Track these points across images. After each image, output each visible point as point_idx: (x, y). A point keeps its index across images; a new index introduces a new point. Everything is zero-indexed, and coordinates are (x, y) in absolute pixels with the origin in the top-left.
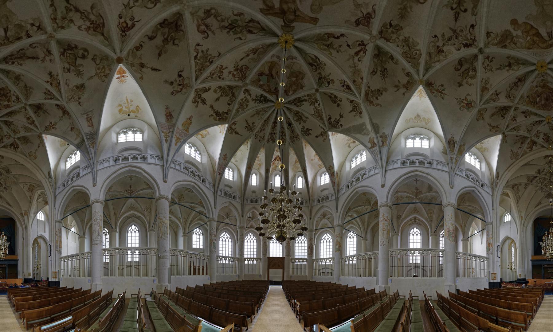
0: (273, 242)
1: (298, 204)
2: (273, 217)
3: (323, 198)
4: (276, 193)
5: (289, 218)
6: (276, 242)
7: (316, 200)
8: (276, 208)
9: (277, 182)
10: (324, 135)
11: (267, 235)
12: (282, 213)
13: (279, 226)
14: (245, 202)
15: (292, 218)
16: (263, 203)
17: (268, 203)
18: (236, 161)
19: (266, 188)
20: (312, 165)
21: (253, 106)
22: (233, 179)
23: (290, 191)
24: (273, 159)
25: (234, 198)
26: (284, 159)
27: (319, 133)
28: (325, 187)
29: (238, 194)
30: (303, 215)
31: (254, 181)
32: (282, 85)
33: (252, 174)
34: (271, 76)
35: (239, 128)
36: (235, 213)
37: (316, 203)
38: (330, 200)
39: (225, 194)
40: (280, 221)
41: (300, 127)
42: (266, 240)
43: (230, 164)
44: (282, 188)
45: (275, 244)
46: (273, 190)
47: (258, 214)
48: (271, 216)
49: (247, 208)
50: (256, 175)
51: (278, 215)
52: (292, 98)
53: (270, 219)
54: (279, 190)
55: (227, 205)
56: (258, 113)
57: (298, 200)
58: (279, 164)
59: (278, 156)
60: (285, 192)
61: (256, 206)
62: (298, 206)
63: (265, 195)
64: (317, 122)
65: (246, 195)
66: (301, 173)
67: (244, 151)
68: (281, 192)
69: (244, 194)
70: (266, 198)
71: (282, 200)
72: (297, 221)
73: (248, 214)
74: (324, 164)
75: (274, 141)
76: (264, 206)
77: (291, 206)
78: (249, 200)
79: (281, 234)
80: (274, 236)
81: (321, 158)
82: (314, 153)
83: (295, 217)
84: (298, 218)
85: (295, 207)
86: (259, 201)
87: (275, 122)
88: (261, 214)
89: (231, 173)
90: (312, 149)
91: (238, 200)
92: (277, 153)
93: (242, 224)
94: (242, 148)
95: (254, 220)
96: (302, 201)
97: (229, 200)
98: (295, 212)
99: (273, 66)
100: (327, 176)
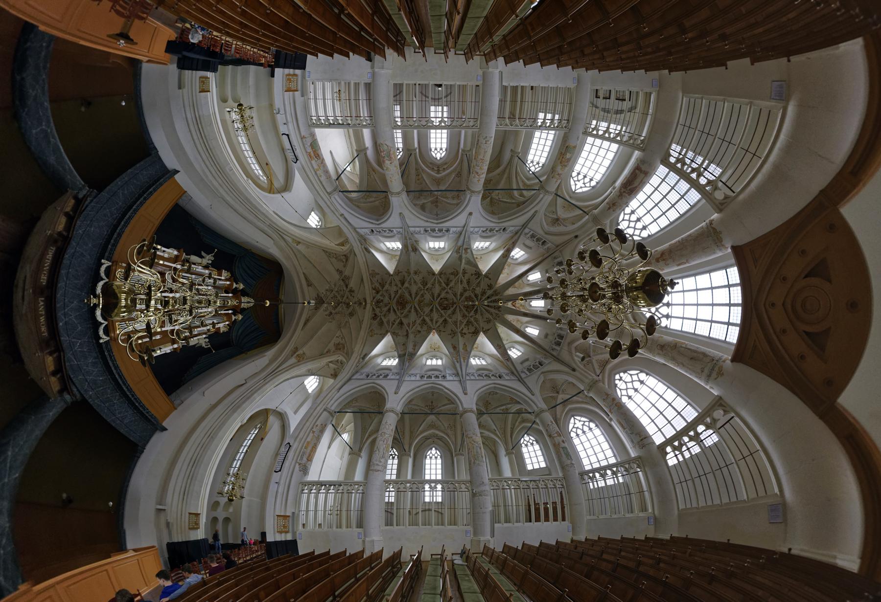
0: (667, 316)
1: (564, 269)
2: (595, 312)
3: (537, 241)
4: (552, 305)
5: (593, 278)
6: (668, 305)
7: (546, 247)
8: (577, 305)
9: (538, 304)
10: (486, 276)
11: (639, 333)
12: (586, 293)
13: (617, 299)
14: (554, 353)
15: (592, 272)
16: (566, 327)
17: (568, 319)
18: (507, 340)
19: (545, 319)
20: (512, 272)
21: (478, 316)
22: (521, 352)
23: (548, 287)
24: (514, 308)
25: (541, 364)
26: (514, 298)
27: (488, 279)
28: (524, 248)
29: (540, 357)
30: (577, 253)
31: (533, 331)
32: (471, 303)
33: (526, 331)
34: (467, 307)
35: (486, 327)
36: (560, 378)
37: (549, 245)
38: (532, 232)
39: (529, 370)
40: (604, 297)
41: (489, 291)
42: (653, 340)
43: (506, 346)
44: (546, 297)
45: (676, 311)
46: (549, 310)
47: (582, 341)
48: (591, 316)
49: (565, 356)
50: (527, 327)
51: (590, 301)
52: (475, 299)
53: (598, 319)
54: (549, 301)
55: (542, 378)
56: (482, 315)
57: (558, 272)
58: (519, 303)
59: (512, 304)
60: (550, 293)
61: (568, 340)
62: (567, 268)
63: (555, 321)
64: (482, 283)
65: (547, 348)
66: (524, 279)
67: (503, 331)
68: (551, 298)
69: (544, 349)
70: (559, 321)
71: (564, 296)
72: (596, 259)
73: (576, 358)
74: (505, 263)
75: (500, 307)
76: (572, 326)
77: (571, 280)
78: (554, 347)
79: (637, 289)
80: (647, 312)
81: (503, 268)
82: (502, 276)
83: (587, 265)
84: (587, 259)
85: (570, 273)
86: (562, 333)
87: (488, 306)
88: (585, 335)
89: (514, 350)
90: (500, 278)
91: (546, 361)
92: (509, 305)
93: (587, 381)
94: (499, 331)
95: (592, 354)
96: (557, 265)
97: (539, 373)
98: (578, 268)
99: (464, 306)
100: (513, 253)
